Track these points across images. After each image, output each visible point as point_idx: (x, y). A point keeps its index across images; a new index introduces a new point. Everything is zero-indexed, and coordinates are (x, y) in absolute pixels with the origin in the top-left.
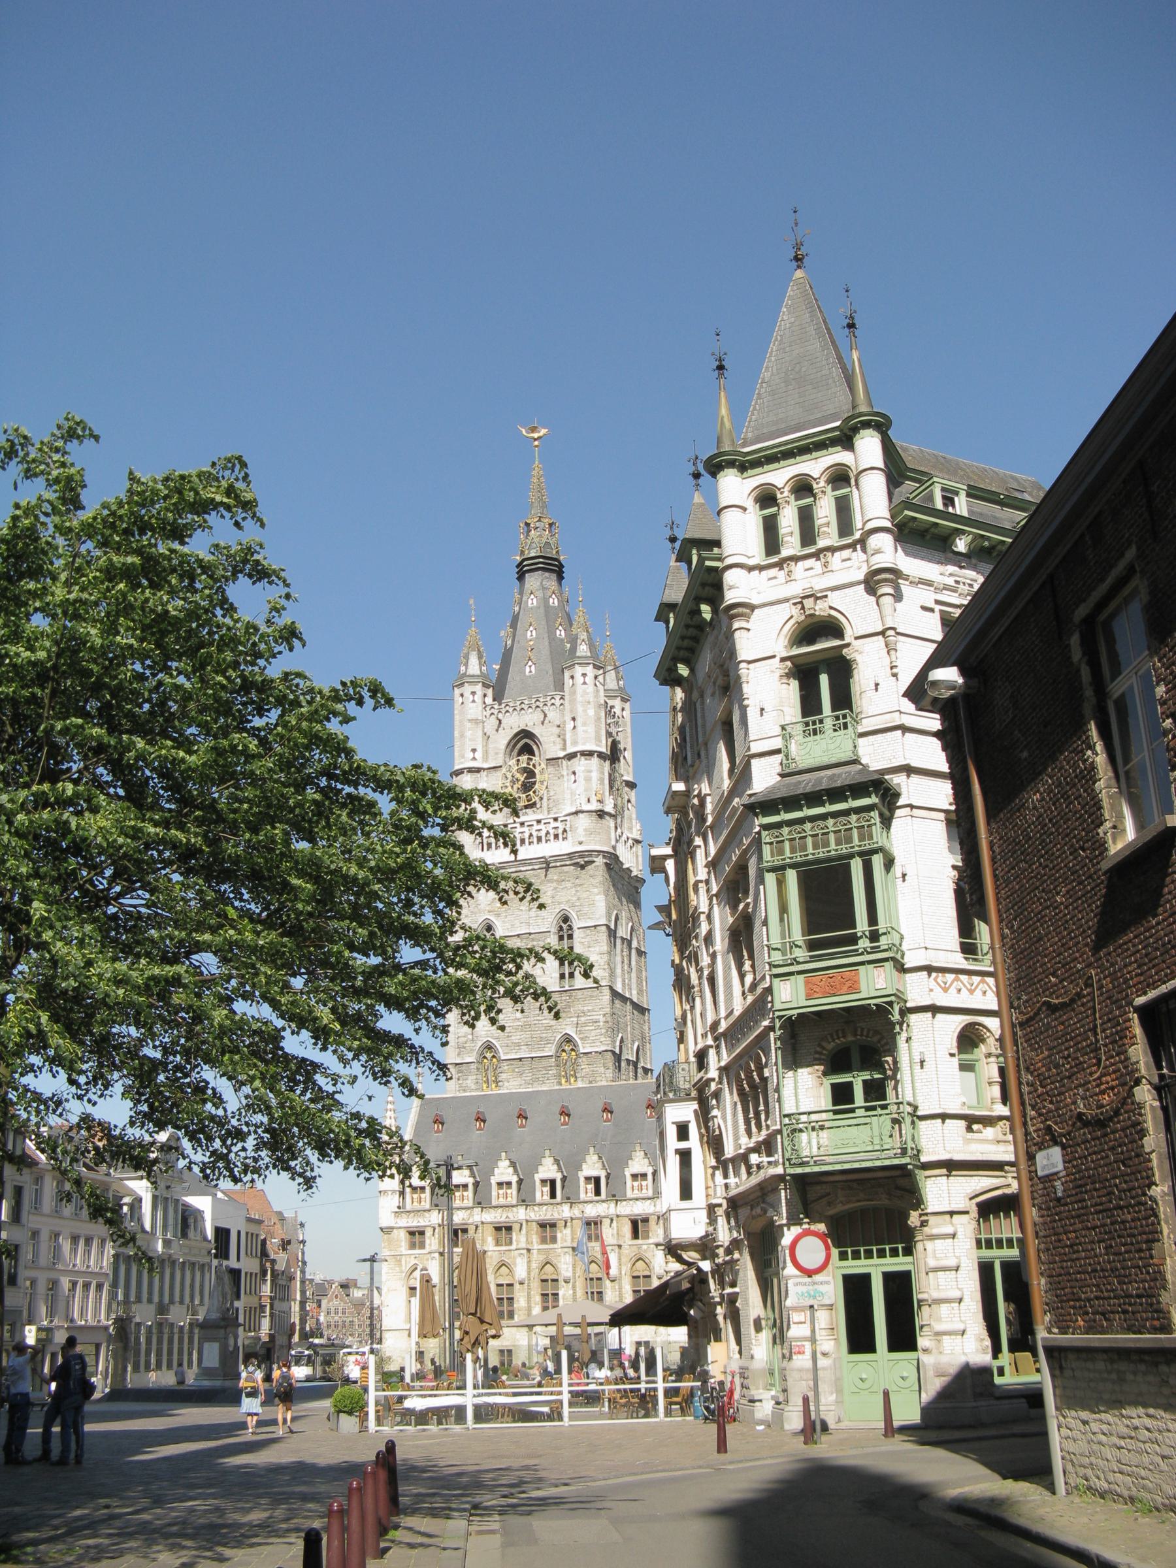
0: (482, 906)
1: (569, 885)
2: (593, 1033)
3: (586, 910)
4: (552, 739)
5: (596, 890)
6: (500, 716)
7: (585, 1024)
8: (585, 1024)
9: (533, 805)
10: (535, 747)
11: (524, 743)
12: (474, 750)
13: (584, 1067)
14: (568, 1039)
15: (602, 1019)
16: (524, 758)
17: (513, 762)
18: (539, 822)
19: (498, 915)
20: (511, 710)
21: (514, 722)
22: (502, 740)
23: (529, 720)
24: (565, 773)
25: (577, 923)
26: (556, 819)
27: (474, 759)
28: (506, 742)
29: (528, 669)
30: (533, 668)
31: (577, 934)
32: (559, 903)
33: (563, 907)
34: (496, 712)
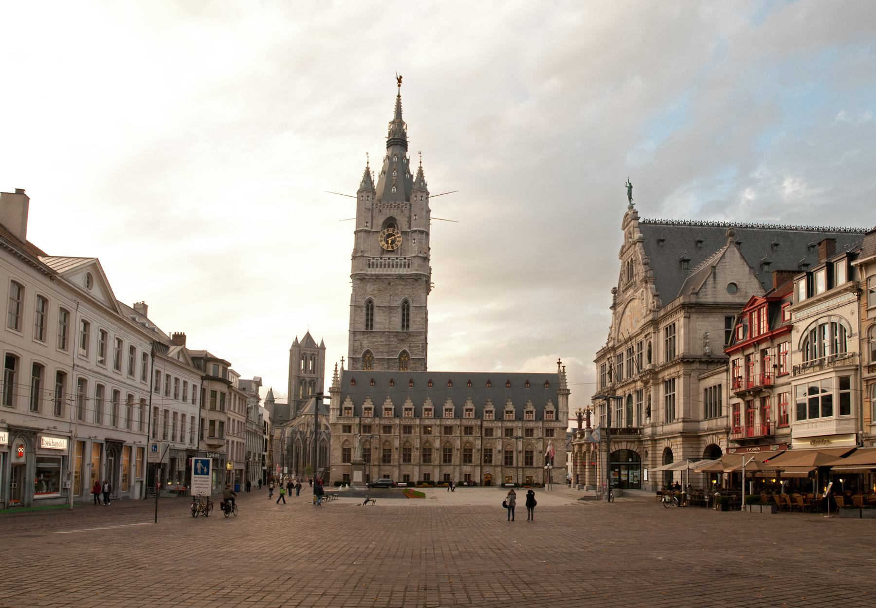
0: (368, 292)
1: (409, 287)
2: (416, 351)
3: (416, 299)
4: (405, 223)
5: (421, 291)
6: (381, 209)
7: (413, 347)
8: (413, 347)
9: (393, 251)
10: (396, 226)
11: (390, 223)
12: (367, 223)
13: (412, 364)
14: (404, 351)
15: (421, 345)
16: (391, 230)
17: (386, 230)
18: (397, 258)
19: (375, 297)
20: (386, 207)
21: (387, 213)
22: (380, 220)
23: (394, 213)
24: (410, 239)
25: (412, 304)
26: (405, 258)
27: (367, 226)
28: (383, 221)
29: (393, 190)
30: (395, 190)
31: (411, 309)
32: (404, 295)
33: (406, 296)
34: (378, 207)
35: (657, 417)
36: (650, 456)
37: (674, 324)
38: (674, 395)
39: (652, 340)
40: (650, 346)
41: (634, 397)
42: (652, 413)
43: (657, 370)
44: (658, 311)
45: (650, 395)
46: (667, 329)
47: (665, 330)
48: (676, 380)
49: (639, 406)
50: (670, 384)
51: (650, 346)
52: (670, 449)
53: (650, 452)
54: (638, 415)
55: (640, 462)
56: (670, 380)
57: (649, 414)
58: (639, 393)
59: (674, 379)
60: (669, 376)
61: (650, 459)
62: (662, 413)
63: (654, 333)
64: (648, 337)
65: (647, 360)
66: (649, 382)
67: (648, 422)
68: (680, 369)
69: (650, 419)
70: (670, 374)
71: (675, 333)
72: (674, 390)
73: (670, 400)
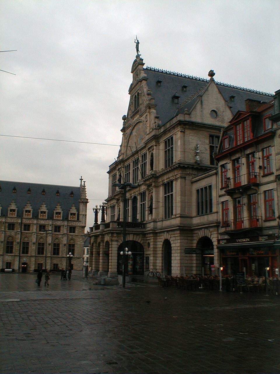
35: (157, 214)
36: (152, 246)
37: (172, 138)
38: (172, 195)
39: (154, 152)
40: (152, 156)
41: (139, 198)
42: (154, 211)
43: (158, 175)
44: (159, 129)
45: (152, 196)
46: (166, 142)
47: (164, 143)
48: (174, 183)
49: (143, 206)
50: (169, 186)
51: (152, 156)
52: (169, 241)
53: (152, 243)
54: (141, 213)
55: (144, 252)
56: (168, 183)
57: (151, 213)
58: (143, 195)
59: (172, 182)
60: (168, 180)
61: (152, 249)
62: (161, 210)
63: (156, 145)
64: (151, 150)
65: (150, 167)
66: (152, 185)
67: (150, 218)
68: (178, 173)
69: (152, 216)
70: (169, 178)
71: (172, 144)
72: (172, 191)
73: (169, 200)
